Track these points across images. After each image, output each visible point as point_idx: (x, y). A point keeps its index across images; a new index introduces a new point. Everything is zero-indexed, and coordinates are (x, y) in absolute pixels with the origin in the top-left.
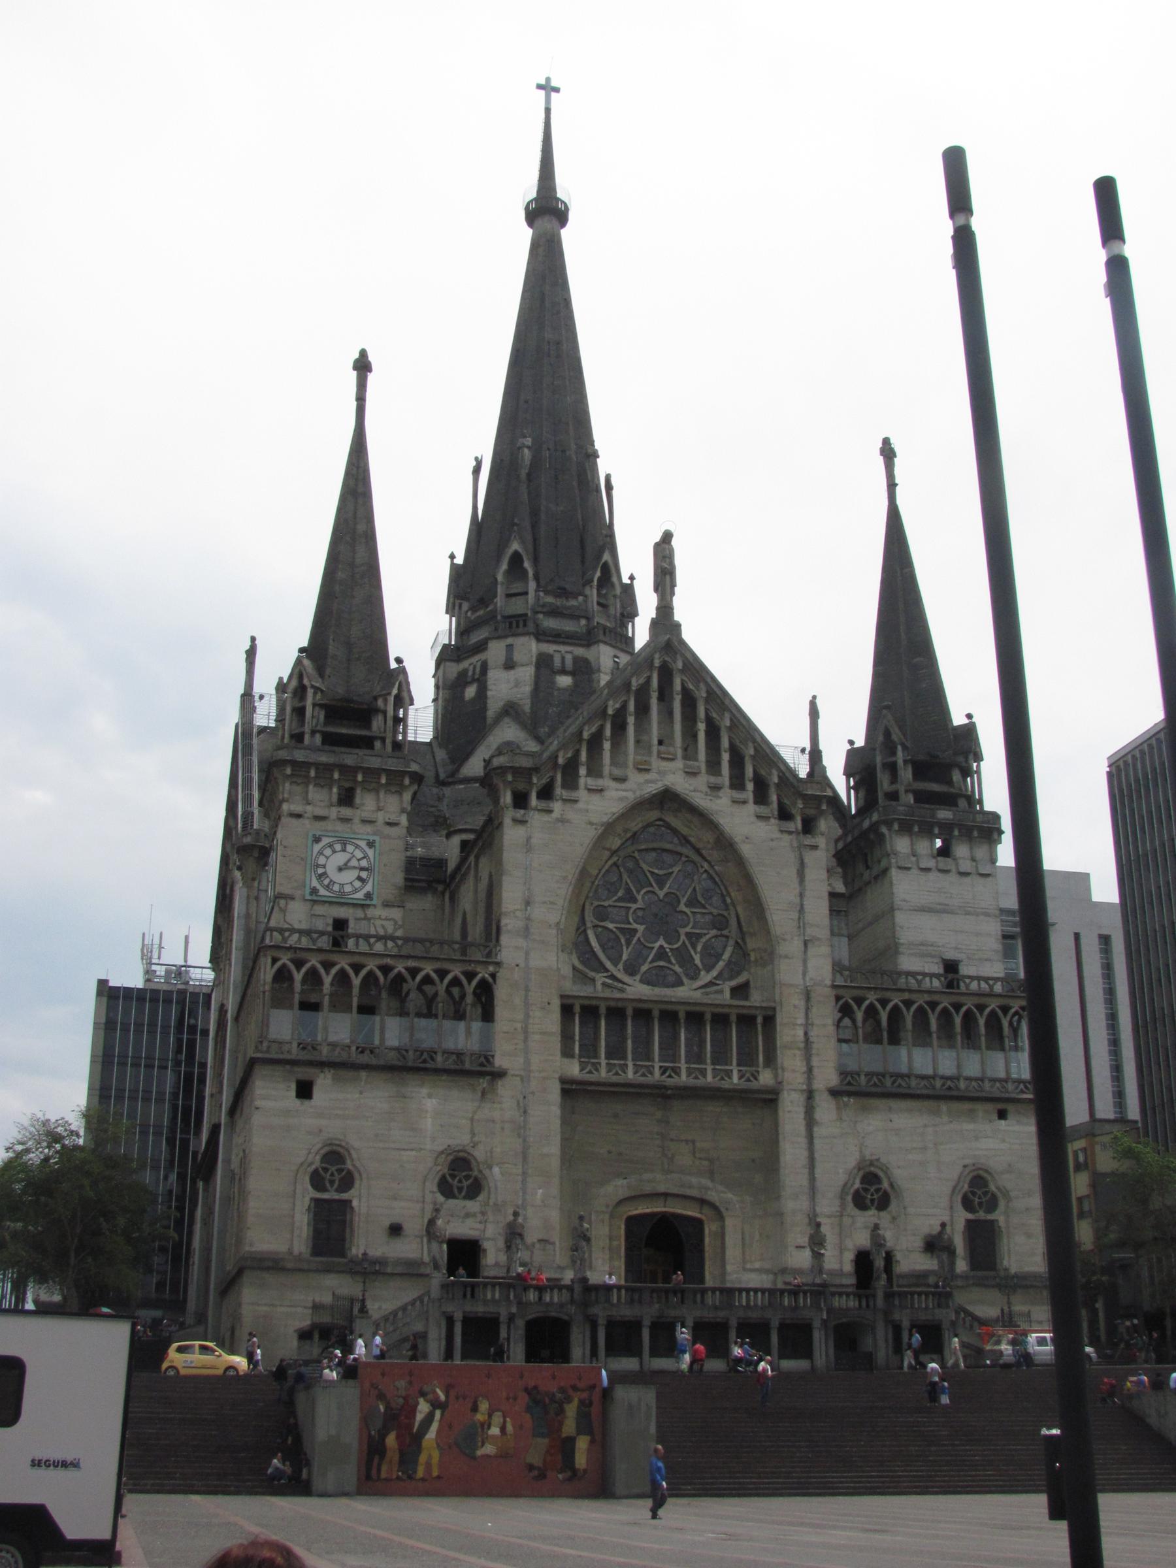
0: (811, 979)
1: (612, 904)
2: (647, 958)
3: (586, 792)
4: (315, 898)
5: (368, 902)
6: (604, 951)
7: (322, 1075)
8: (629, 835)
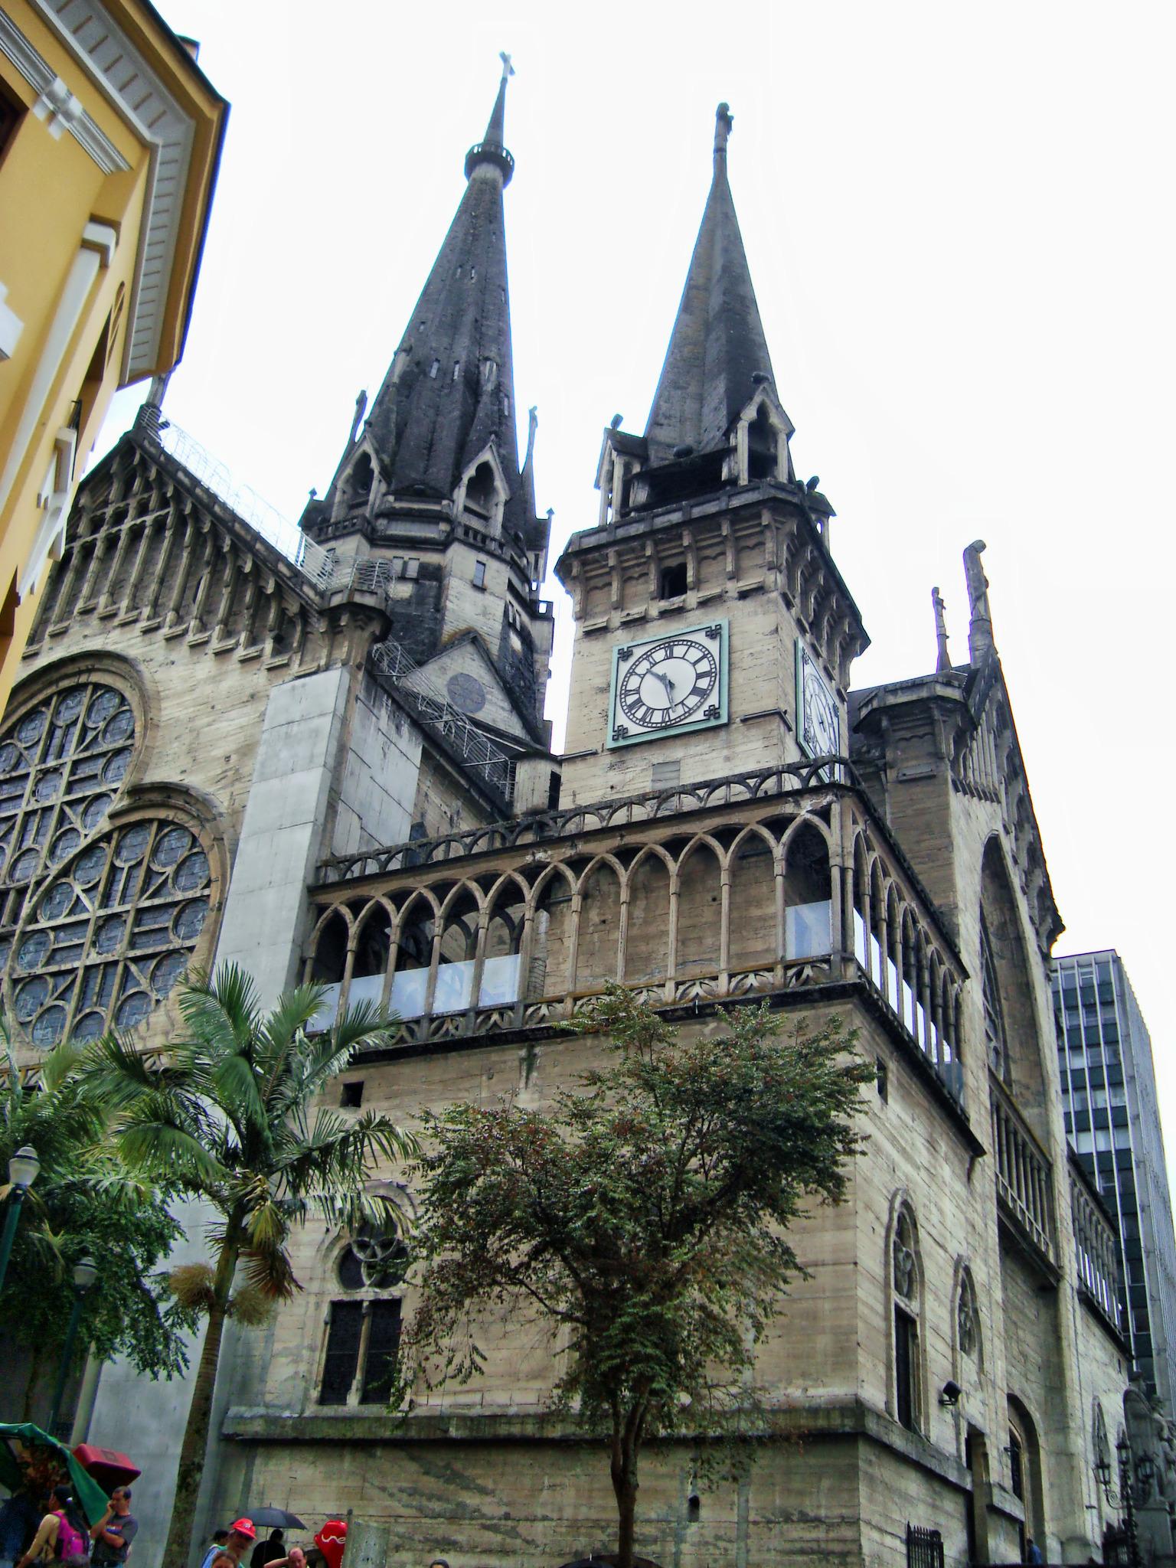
4: (622, 743)
5: (713, 723)
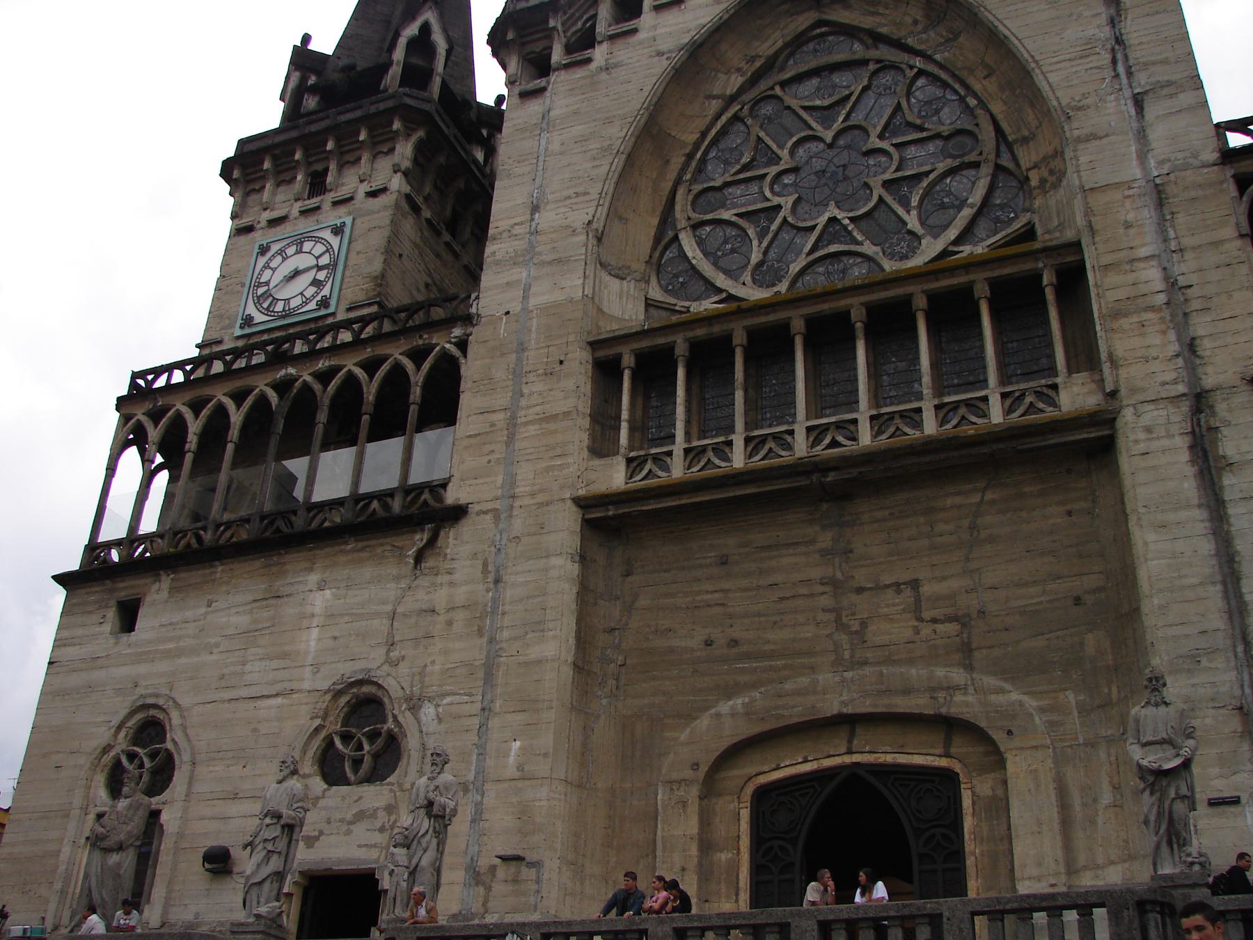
0: (1161, 163)
1: (729, 179)
2: (801, 251)
3: (653, 13)
4: (247, 331)
5: (323, 312)
6: (715, 264)
7: (156, 586)
8: (758, 64)
